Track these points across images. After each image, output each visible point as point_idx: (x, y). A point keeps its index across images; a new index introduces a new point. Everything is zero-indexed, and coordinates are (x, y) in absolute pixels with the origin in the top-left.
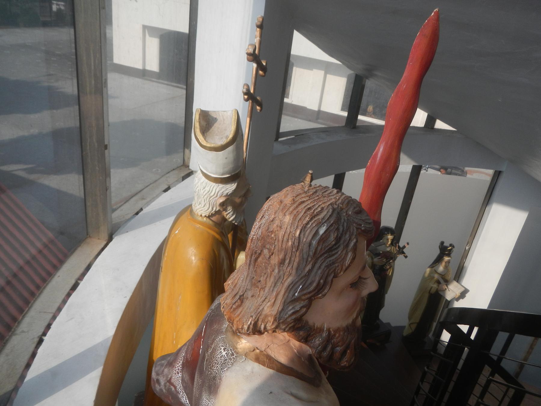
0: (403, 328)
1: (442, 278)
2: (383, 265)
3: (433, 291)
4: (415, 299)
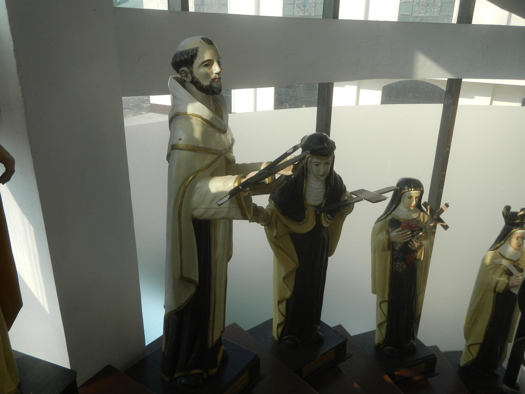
0: (460, 353)
1: (515, 266)
2: (408, 243)
3: (501, 288)
4: (471, 304)
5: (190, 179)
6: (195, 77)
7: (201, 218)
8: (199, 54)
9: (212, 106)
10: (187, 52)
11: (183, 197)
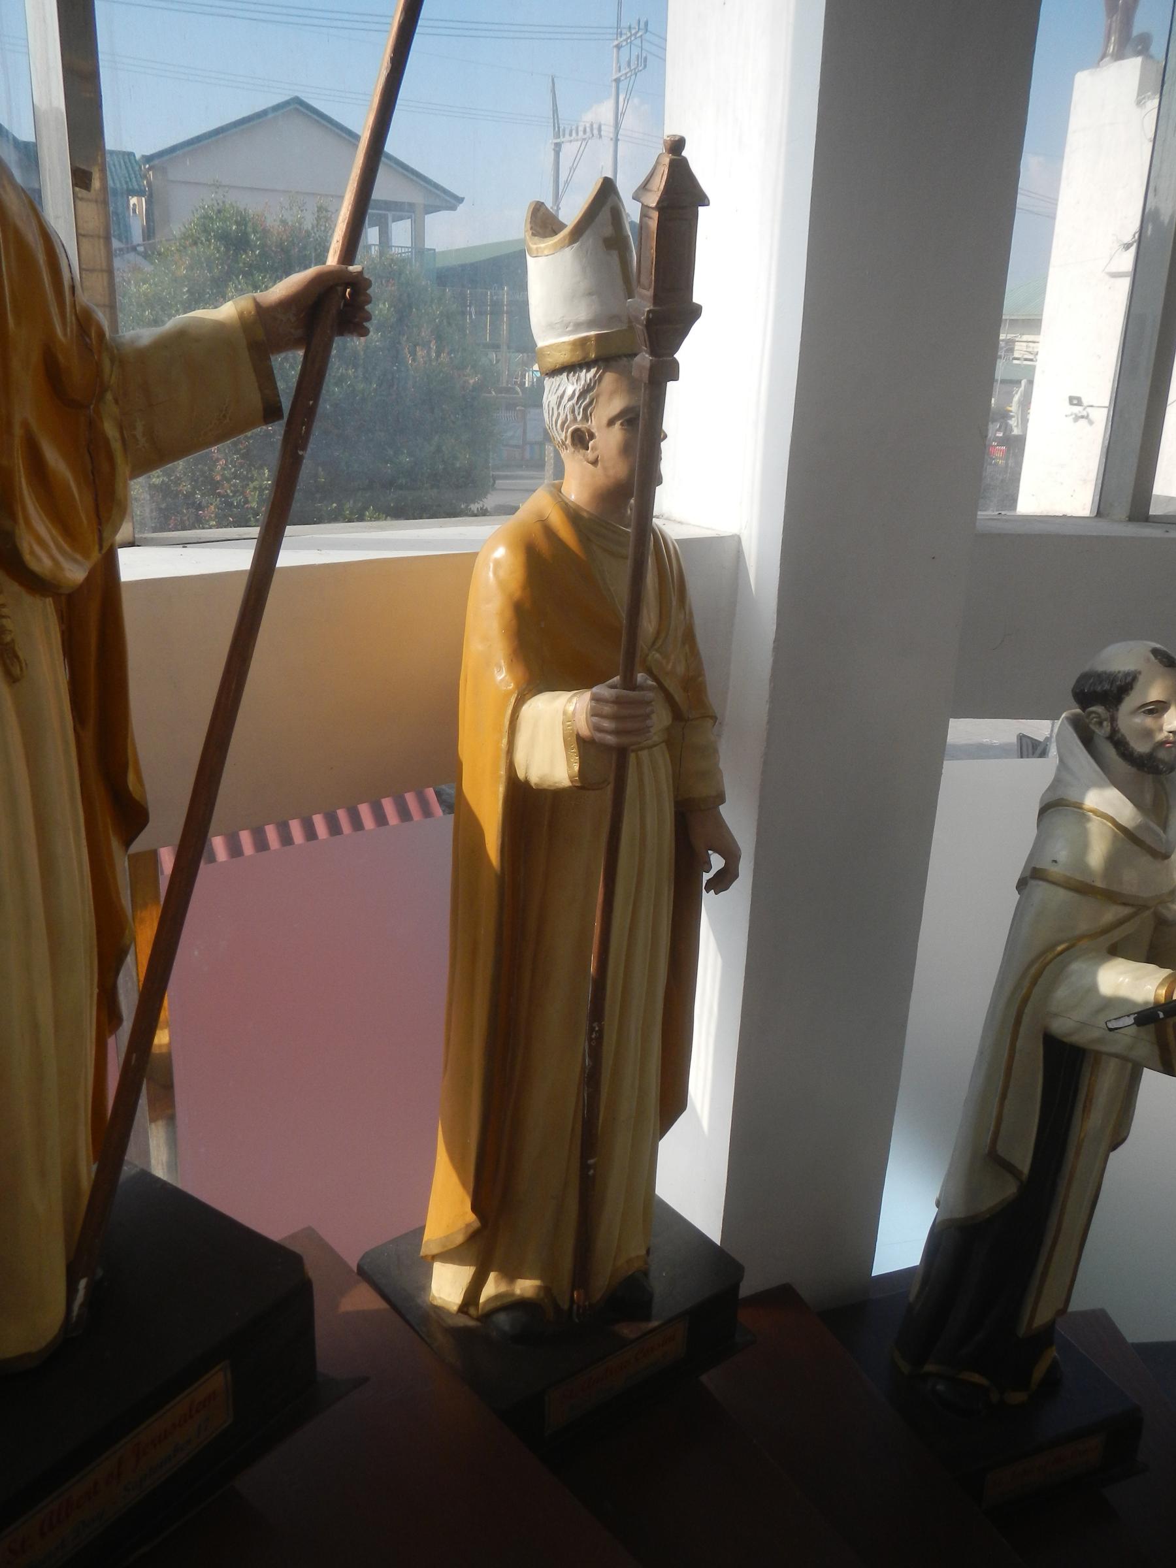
5: (1060, 948)
6: (1119, 731)
7: (1065, 1040)
8: (1138, 686)
9: (1148, 798)
10: (1111, 677)
11: (1034, 982)
